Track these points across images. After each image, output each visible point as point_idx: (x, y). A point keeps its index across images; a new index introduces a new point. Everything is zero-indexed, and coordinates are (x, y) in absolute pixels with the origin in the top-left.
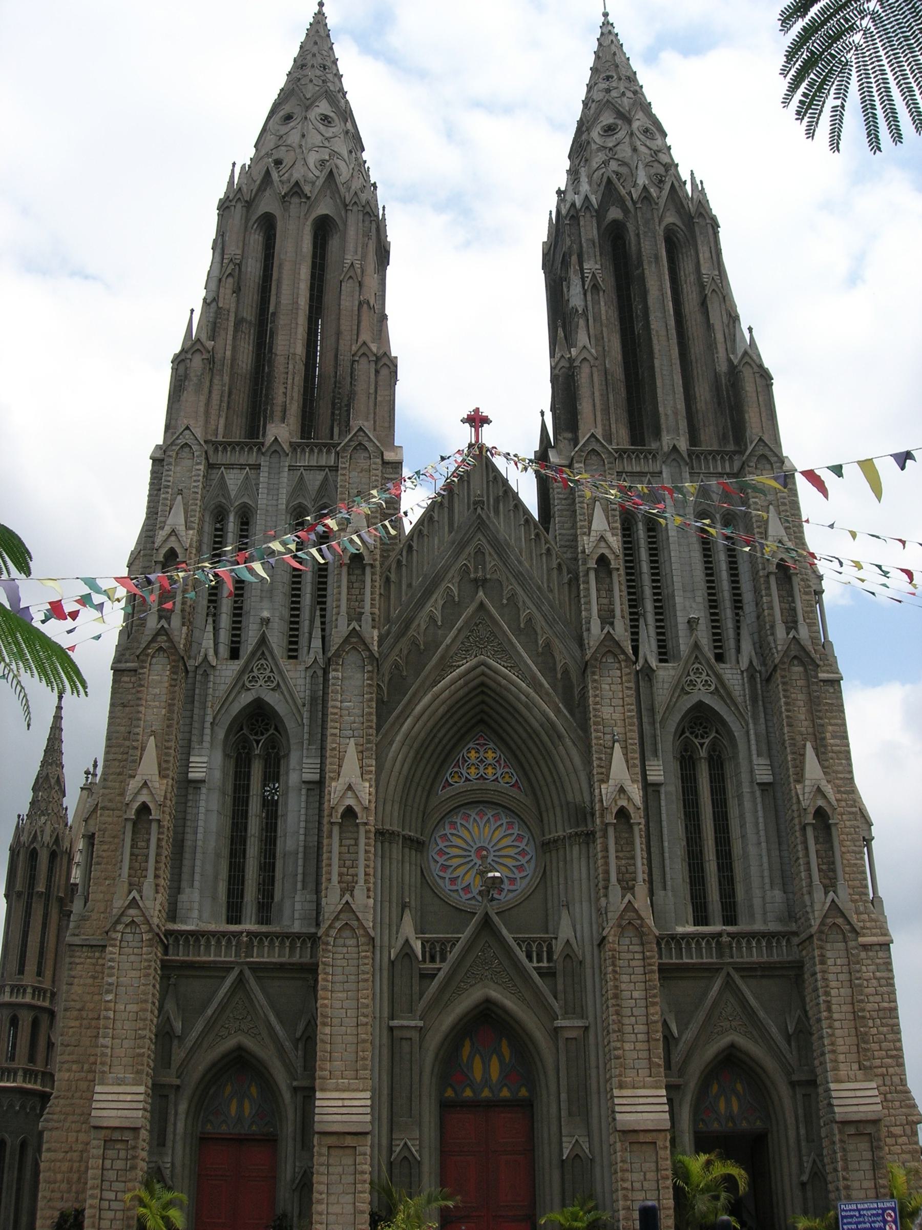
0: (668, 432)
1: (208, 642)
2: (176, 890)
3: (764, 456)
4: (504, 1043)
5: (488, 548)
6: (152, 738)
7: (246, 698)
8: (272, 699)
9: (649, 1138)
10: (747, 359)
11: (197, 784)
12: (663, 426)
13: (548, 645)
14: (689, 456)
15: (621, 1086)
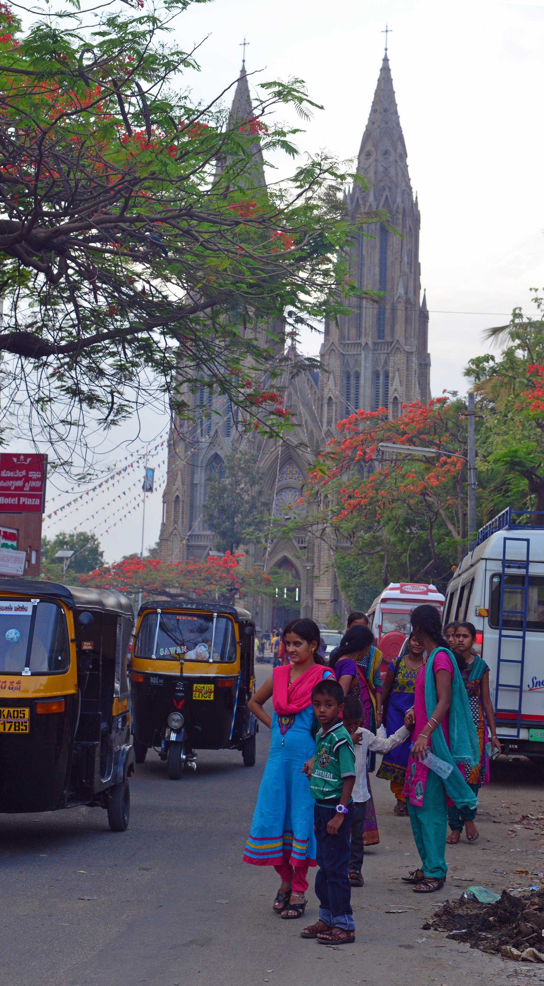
0: (365, 335)
1: (199, 431)
2: (191, 520)
3: (398, 348)
4: (293, 569)
5: (293, 392)
6: (179, 472)
7: (212, 453)
8: (219, 452)
9: (324, 602)
10: (400, 300)
11: (197, 484)
12: (363, 334)
13: (312, 431)
14: (374, 344)
15: (318, 586)
